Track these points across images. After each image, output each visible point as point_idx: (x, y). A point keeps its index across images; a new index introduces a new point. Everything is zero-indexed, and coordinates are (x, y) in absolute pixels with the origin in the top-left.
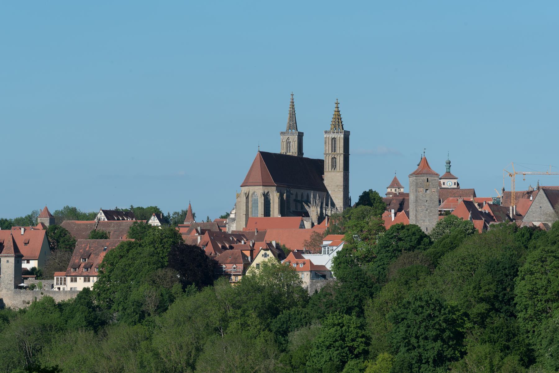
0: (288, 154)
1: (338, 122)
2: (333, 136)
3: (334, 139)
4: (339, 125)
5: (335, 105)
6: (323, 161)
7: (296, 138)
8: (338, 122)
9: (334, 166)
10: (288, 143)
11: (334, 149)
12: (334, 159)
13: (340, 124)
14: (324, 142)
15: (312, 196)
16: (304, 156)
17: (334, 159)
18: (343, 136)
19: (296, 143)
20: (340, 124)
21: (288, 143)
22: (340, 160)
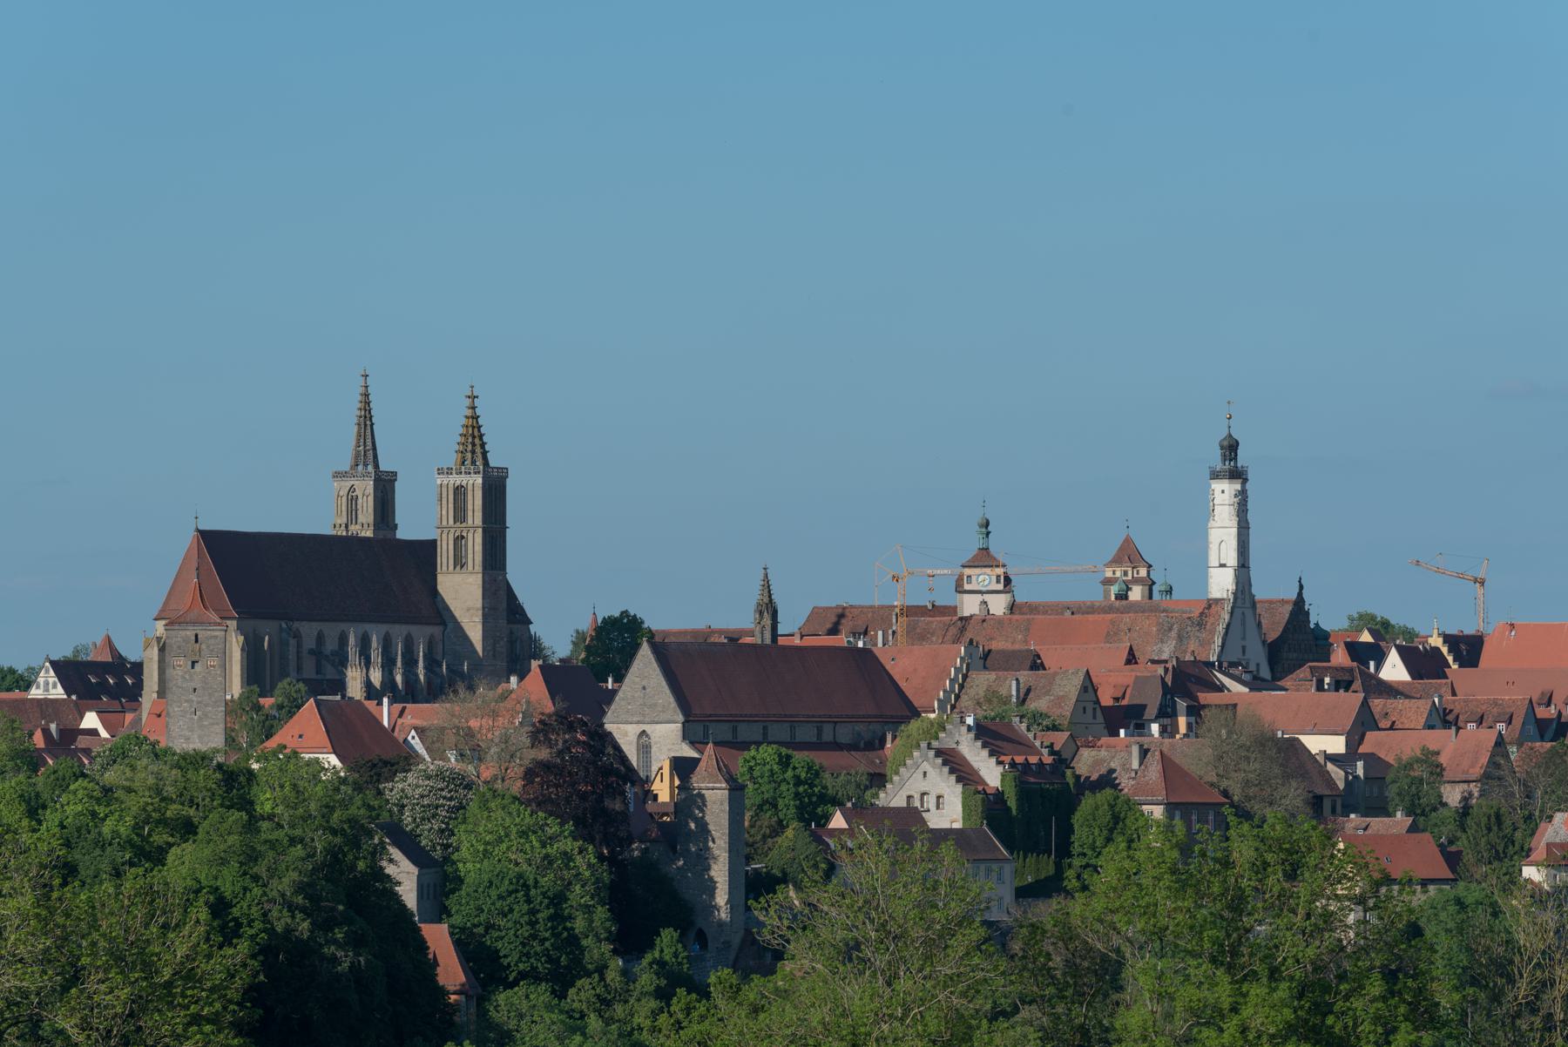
0: (354, 529)
1: (474, 441)
3: (460, 491)
4: (473, 452)
5: (468, 402)
6: (432, 545)
7: (370, 485)
8: (474, 441)
9: (460, 562)
10: (352, 500)
11: (460, 514)
12: (459, 539)
13: (478, 450)
14: (436, 497)
15: (352, 640)
16: (403, 533)
17: (459, 539)
18: (479, 480)
19: (371, 499)
20: (478, 450)
21: (352, 500)
22: (475, 543)
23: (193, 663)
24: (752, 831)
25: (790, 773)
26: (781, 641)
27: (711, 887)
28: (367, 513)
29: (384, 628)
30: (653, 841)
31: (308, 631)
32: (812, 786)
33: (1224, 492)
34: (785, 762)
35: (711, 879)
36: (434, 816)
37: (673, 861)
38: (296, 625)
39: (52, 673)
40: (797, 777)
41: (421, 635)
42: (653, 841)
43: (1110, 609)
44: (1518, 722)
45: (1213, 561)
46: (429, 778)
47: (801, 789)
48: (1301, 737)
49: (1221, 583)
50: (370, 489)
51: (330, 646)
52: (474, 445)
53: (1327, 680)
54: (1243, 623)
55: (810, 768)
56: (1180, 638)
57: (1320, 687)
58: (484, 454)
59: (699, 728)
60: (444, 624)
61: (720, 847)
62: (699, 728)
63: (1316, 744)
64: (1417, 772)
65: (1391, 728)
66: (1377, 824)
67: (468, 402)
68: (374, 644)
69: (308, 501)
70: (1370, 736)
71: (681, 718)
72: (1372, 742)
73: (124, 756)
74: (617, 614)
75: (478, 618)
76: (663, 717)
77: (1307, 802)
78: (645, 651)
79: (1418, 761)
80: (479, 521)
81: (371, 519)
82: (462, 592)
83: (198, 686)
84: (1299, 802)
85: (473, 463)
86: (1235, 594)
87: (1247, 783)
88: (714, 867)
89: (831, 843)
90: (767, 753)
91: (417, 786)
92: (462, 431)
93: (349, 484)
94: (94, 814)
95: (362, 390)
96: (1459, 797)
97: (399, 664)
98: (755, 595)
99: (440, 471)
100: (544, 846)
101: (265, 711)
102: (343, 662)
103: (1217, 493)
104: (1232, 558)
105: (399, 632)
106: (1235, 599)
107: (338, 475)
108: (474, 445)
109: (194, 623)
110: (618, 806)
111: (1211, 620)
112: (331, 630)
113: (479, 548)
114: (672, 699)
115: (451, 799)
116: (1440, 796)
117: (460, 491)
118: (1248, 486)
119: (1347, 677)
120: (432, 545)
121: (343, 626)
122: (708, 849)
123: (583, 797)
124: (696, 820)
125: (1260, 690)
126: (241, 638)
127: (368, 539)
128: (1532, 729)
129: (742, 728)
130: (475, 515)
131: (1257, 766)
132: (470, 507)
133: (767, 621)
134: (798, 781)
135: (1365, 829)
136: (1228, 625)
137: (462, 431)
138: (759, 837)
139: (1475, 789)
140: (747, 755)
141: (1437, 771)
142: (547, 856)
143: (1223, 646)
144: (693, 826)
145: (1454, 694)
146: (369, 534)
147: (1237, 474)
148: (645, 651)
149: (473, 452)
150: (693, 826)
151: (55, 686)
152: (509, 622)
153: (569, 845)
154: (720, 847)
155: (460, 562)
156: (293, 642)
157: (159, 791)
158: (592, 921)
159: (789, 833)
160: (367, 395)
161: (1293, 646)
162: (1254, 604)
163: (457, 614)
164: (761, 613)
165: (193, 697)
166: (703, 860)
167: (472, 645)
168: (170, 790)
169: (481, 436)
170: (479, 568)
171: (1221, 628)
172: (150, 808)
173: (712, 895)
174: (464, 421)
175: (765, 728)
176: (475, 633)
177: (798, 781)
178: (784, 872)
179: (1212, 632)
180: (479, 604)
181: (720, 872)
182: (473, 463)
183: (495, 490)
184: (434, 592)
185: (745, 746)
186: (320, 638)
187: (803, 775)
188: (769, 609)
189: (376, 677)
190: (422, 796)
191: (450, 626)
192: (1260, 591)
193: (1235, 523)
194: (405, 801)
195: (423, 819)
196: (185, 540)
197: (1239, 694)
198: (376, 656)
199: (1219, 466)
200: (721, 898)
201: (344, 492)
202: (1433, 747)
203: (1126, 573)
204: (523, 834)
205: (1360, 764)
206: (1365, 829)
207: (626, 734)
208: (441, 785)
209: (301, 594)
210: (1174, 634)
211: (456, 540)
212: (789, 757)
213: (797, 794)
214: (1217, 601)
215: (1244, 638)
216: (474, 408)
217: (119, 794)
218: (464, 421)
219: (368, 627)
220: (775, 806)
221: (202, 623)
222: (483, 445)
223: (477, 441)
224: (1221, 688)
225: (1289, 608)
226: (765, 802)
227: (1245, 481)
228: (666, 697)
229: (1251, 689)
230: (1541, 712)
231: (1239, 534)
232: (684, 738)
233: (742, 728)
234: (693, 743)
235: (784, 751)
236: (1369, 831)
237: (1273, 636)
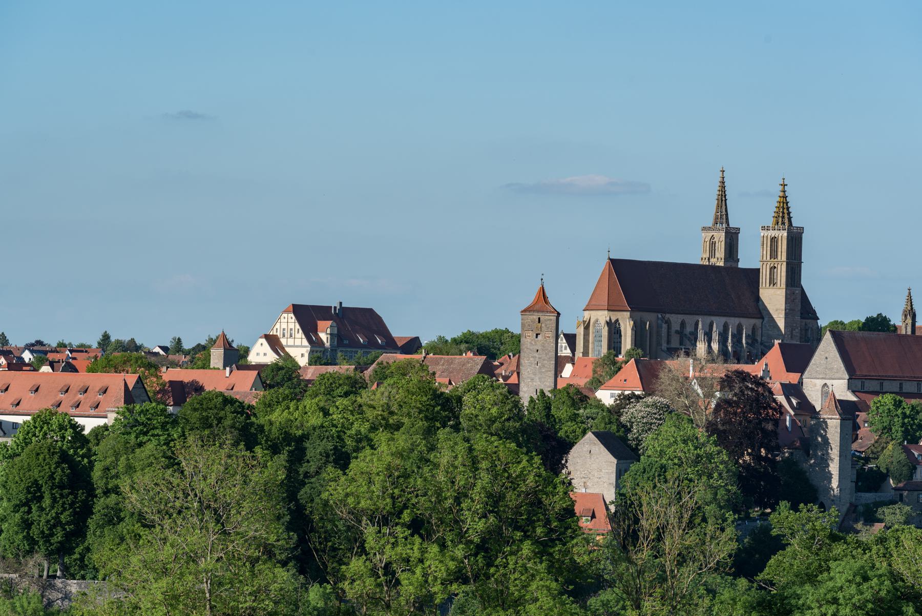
0: (713, 261)
1: (784, 212)
2: (772, 233)
3: (774, 240)
4: (783, 217)
5: (781, 188)
7: (722, 235)
8: (784, 212)
10: (713, 245)
11: (774, 254)
13: (786, 216)
14: (760, 243)
16: (741, 265)
18: (785, 234)
19: (723, 243)
20: (786, 216)
21: (713, 245)
23: (537, 335)
24: (876, 445)
25: (900, 411)
26: (918, 333)
27: (829, 477)
28: (720, 253)
29: (723, 320)
30: (796, 449)
31: (676, 320)
32: (913, 419)
34: (898, 404)
35: (829, 472)
36: (649, 429)
37: (807, 461)
38: (668, 316)
39: (564, 341)
40: (904, 414)
41: (747, 324)
42: (796, 449)
46: (648, 406)
47: (906, 421)
50: (723, 238)
51: (689, 329)
52: (783, 213)
55: (913, 408)
58: (790, 219)
59: (859, 383)
60: (763, 318)
61: (835, 452)
62: (859, 383)
67: (781, 188)
68: (714, 329)
69: (688, 244)
71: (847, 377)
73: (475, 388)
74: (875, 316)
75: (782, 315)
76: (837, 375)
78: (827, 338)
80: (784, 258)
81: (723, 256)
82: (774, 299)
83: (539, 348)
85: (783, 223)
88: (831, 465)
89: (916, 454)
90: (888, 399)
91: (641, 411)
92: (777, 205)
93: (711, 234)
94: (348, 420)
95: (720, 179)
97: (730, 341)
98: (902, 305)
99: (763, 228)
100: (696, 448)
101: (618, 365)
102: (696, 339)
105: (733, 322)
107: (704, 229)
108: (783, 213)
109: (538, 311)
110: (770, 427)
112: (690, 320)
113: (784, 274)
114: (842, 365)
115: (660, 419)
117: (774, 240)
120: (757, 271)
121: (697, 317)
122: (828, 454)
123: (750, 422)
124: (821, 436)
126: (632, 323)
127: (719, 267)
129: (886, 384)
130: (783, 255)
132: (779, 250)
133: (909, 321)
134: (905, 416)
137: (777, 205)
138: (879, 449)
140: (876, 399)
142: (698, 456)
144: (820, 439)
146: (721, 264)
148: (827, 338)
149: (783, 217)
150: (820, 439)
151: (566, 349)
152: (802, 318)
153: (715, 449)
154: (835, 452)
155: (772, 282)
156: (665, 326)
157: (389, 406)
158: (716, 494)
159: (890, 447)
160: (723, 183)
163: (771, 312)
164: (906, 316)
165: (536, 355)
166: (824, 461)
167: (779, 329)
168: (395, 408)
169: (788, 208)
170: (784, 286)
172: (380, 418)
173: (830, 482)
174: (778, 199)
175: (901, 384)
176: (781, 324)
177: (905, 416)
178: (887, 469)
180: (783, 307)
181: (834, 468)
182: (783, 223)
183: (795, 240)
184: (758, 299)
185: (877, 393)
186: (683, 324)
187: (908, 413)
188: (911, 313)
189: (715, 346)
190: (643, 418)
191: (766, 319)
194: (633, 420)
195: (643, 431)
196: (602, 265)
198: (715, 336)
200: (835, 484)
201: (708, 239)
204: (685, 442)
207: (815, 385)
208: (655, 411)
209: (661, 298)
211: (771, 269)
212: (900, 402)
213: (903, 424)
216: (784, 191)
217: (365, 408)
218: (778, 199)
219: (713, 318)
220: (891, 429)
221: (543, 311)
222: (789, 213)
223: (785, 211)
226: (884, 428)
228: (839, 364)
232: (849, 387)
233: (886, 384)
234: (854, 392)
235: (898, 398)
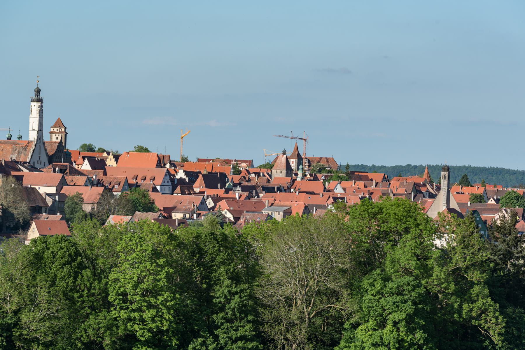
33: (35, 106)
43: (5, 143)
44: (122, 184)
45: (31, 128)
48: (37, 188)
49: (33, 136)
53: (57, 169)
54: (40, 149)
56: (19, 153)
57: (54, 171)
63: (43, 190)
64: (76, 200)
65: (74, 185)
66: (52, 217)
70: (65, 188)
72: (66, 190)
77: (28, 209)
79: (75, 196)
84: (25, 209)
86: (37, 139)
87: (8, 203)
96: (90, 208)
103: (33, 106)
104: (37, 128)
106: (37, 141)
111: (29, 148)
116: (81, 208)
118: (43, 104)
119: (65, 168)
125: (33, 171)
128: (127, 187)
131: (12, 196)
135: (47, 218)
136: (34, 150)
139: (96, 206)
141: (82, 200)
143: (32, 156)
145: (105, 174)
147: (40, 100)
161: (60, 158)
162: (44, 143)
171: (32, 151)
179: (29, 152)
192: (46, 139)
193: (37, 116)
197: (26, 173)
199: (34, 97)
202: (80, 193)
203: (57, 130)
205: (57, 197)
206: (47, 218)
210: (17, 152)
214: (31, 141)
215: (40, 154)
224: (20, 170)
225: (57, 144)
227: (42, 102)
229: (30, 171)
230: (131, 181)
231: (39, 120)
236: (48, 219)
237: (51, 154)
